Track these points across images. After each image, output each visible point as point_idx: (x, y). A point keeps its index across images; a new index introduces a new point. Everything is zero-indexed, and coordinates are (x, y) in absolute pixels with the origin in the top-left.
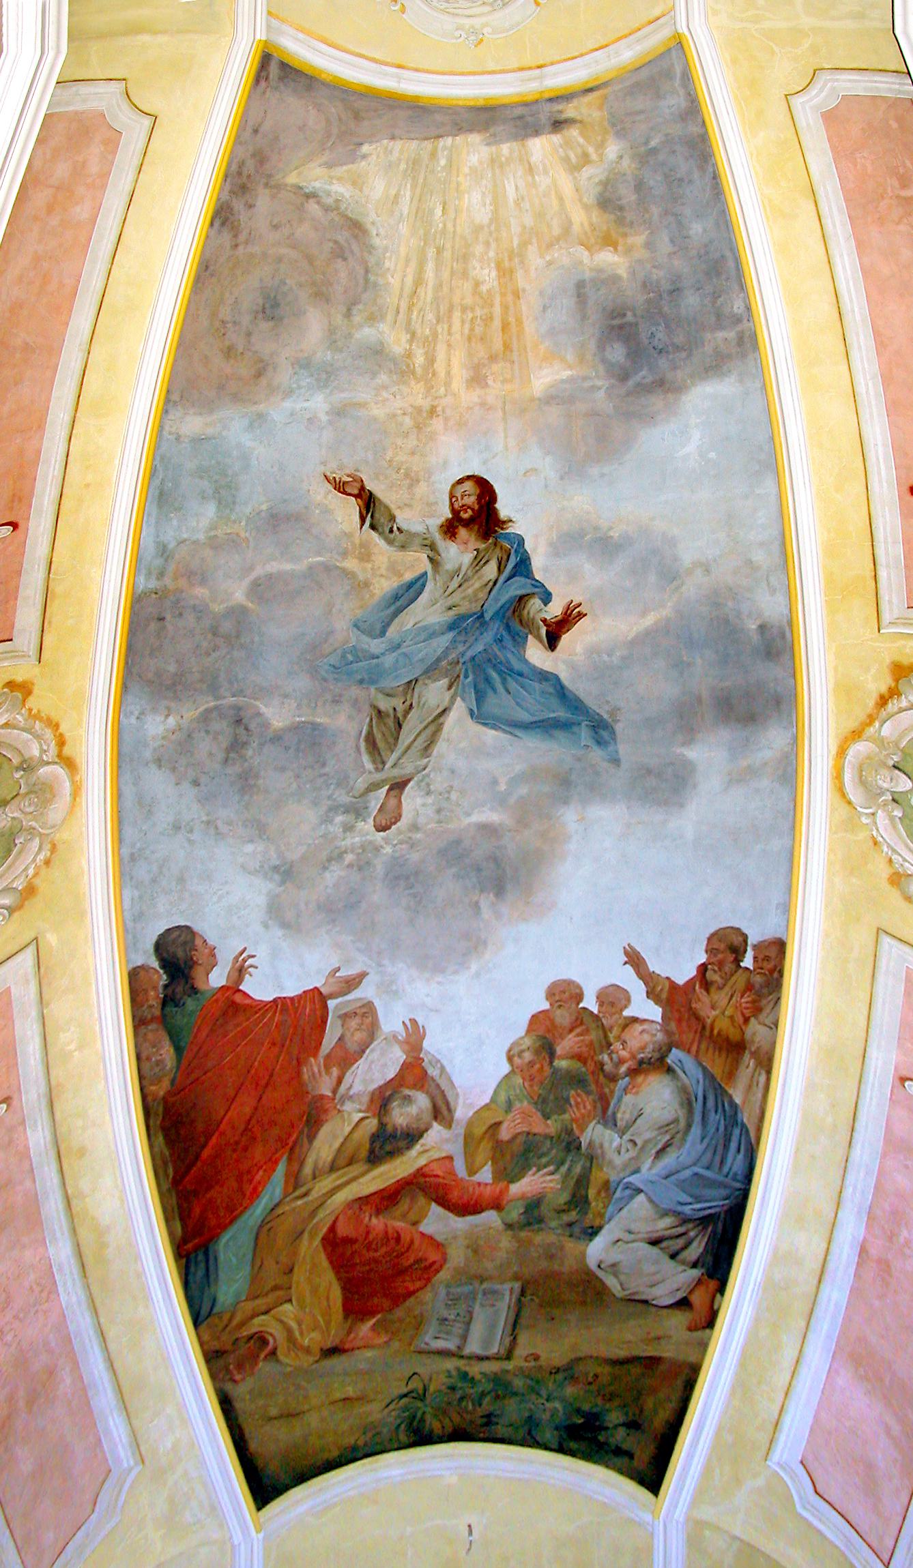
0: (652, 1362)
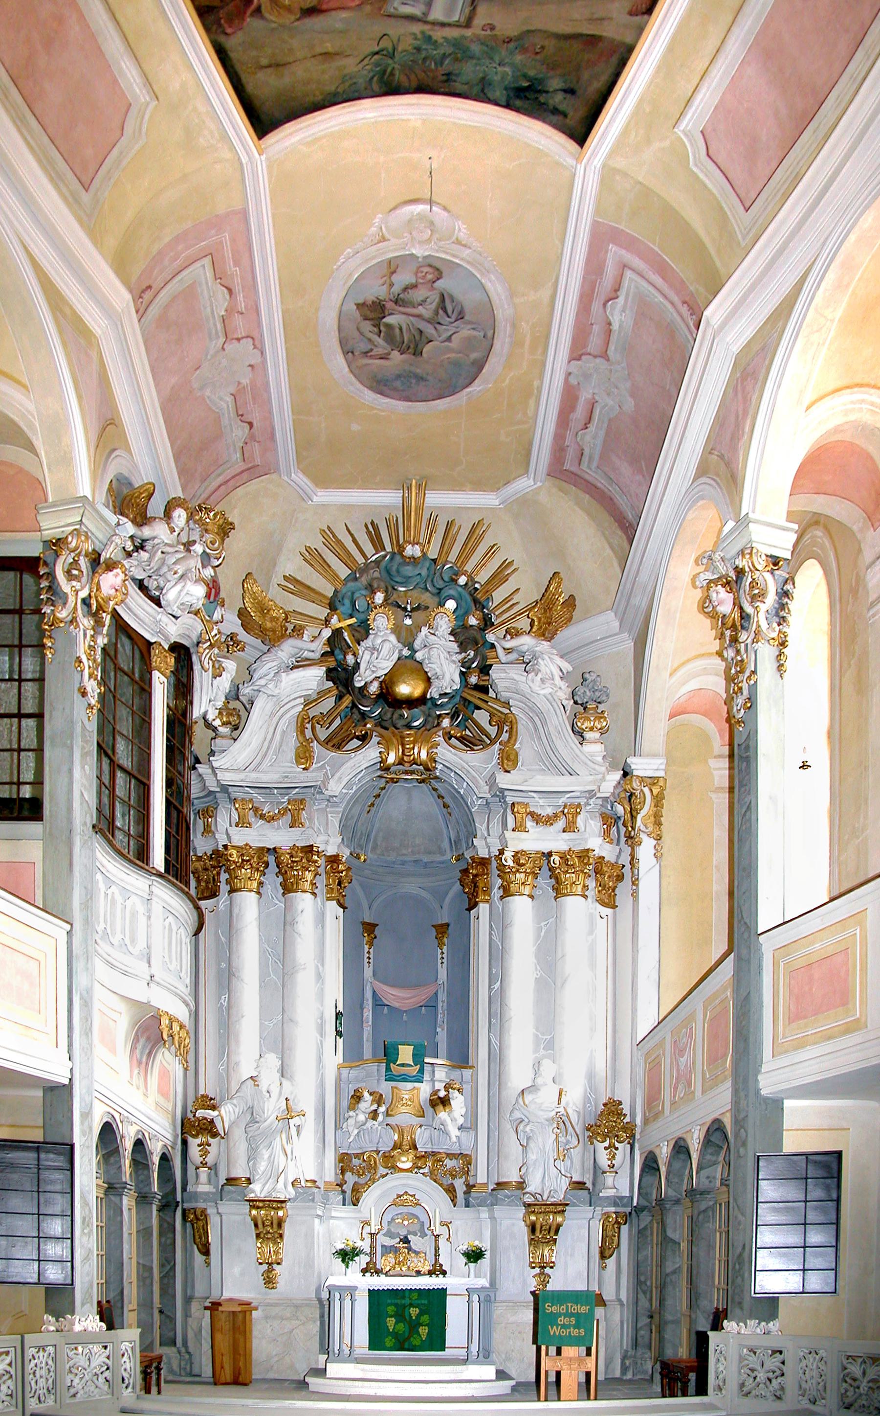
0: (592, 40)
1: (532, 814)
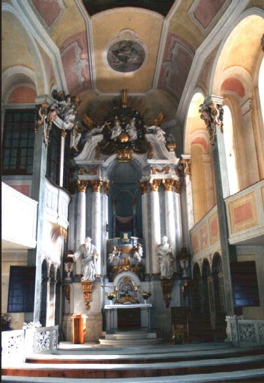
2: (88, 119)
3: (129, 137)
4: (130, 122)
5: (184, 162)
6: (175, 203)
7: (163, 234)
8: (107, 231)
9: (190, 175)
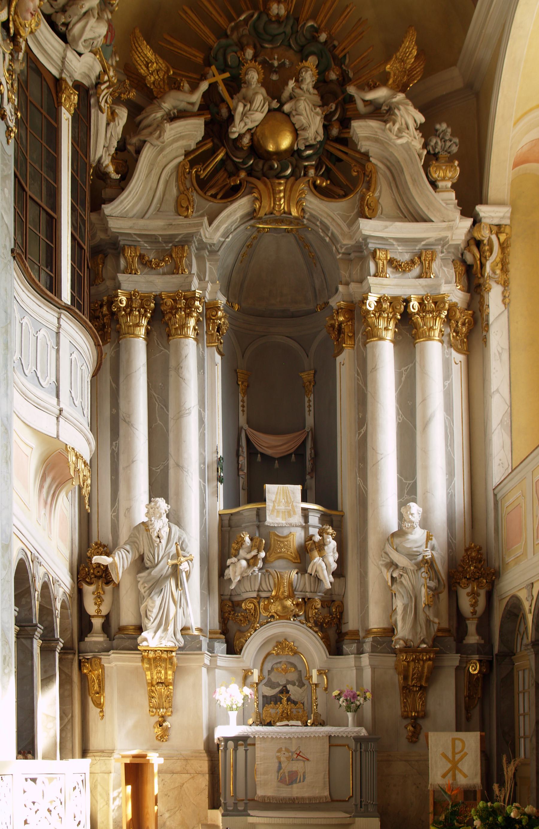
1: (391, 262)
2: (150, 54)
3: (296, 133)
4: (300, 72)
5: (484, 234)
6: (451, 385)
7: (406, 497)
8: (220, 480)
9: (506, 284)
